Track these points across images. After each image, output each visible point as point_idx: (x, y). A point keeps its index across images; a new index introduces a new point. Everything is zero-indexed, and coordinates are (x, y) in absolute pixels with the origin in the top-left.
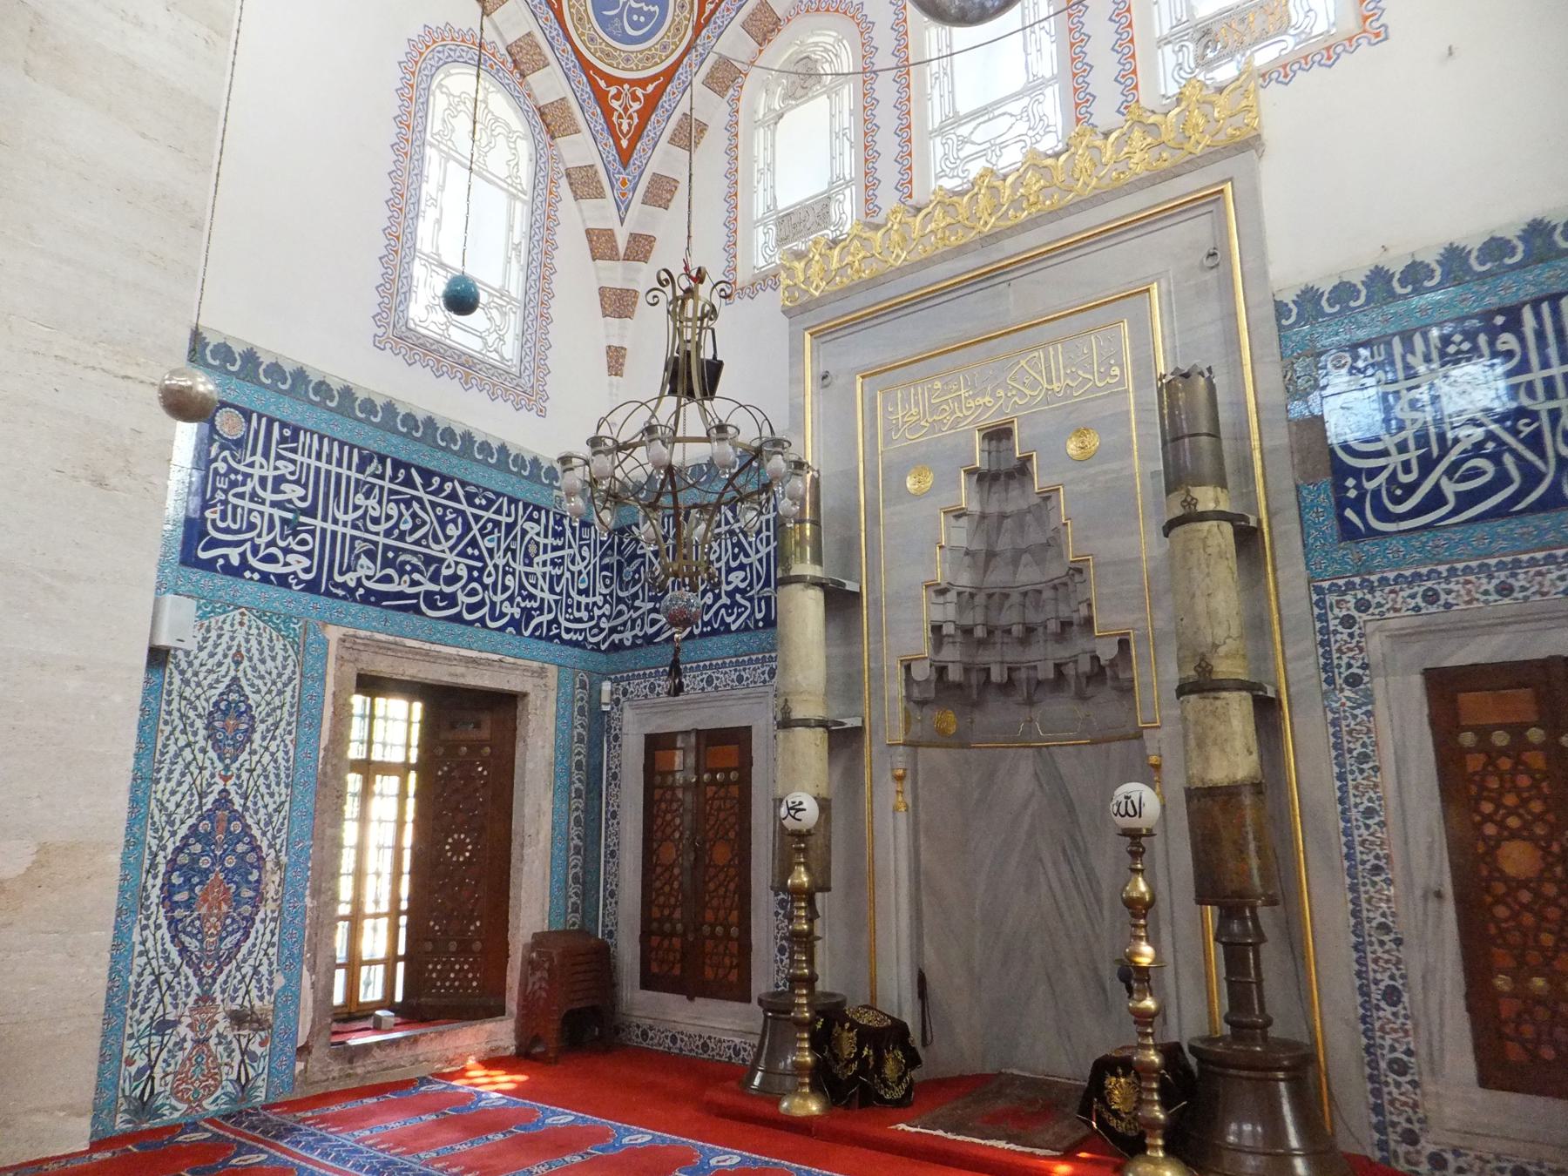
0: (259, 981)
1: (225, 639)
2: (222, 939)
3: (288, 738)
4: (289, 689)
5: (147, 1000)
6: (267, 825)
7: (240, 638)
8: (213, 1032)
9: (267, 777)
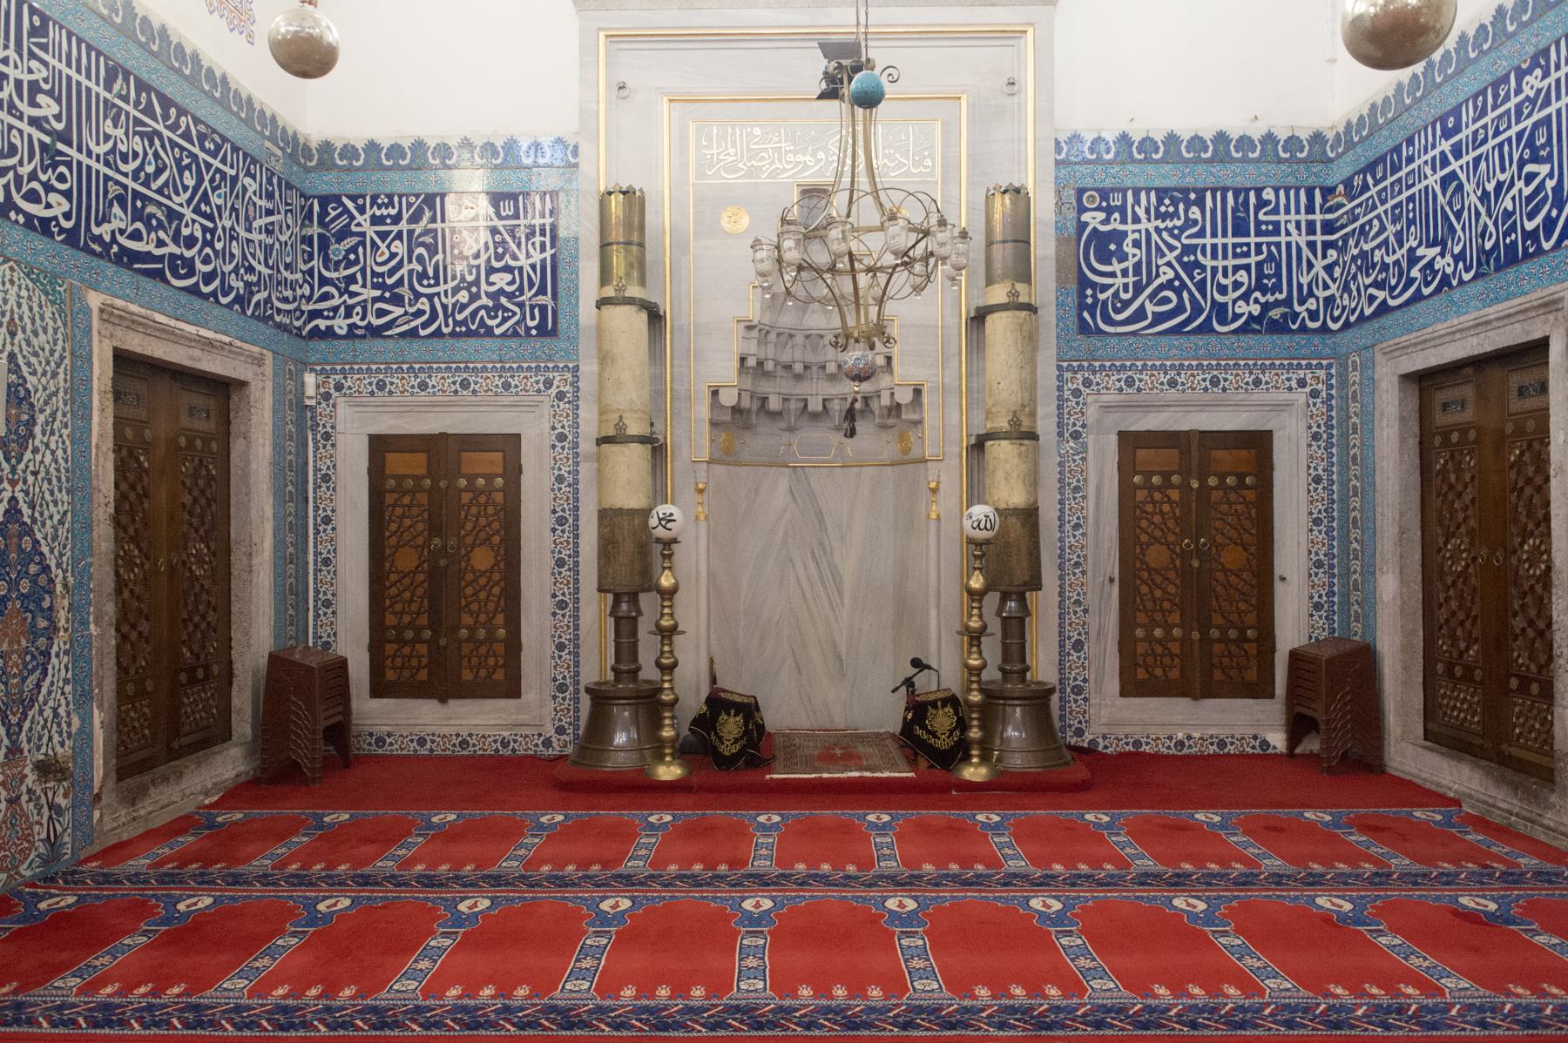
0: (59, 725)
4: (61, 370)
6: (54, 540)
8: (24, 789)
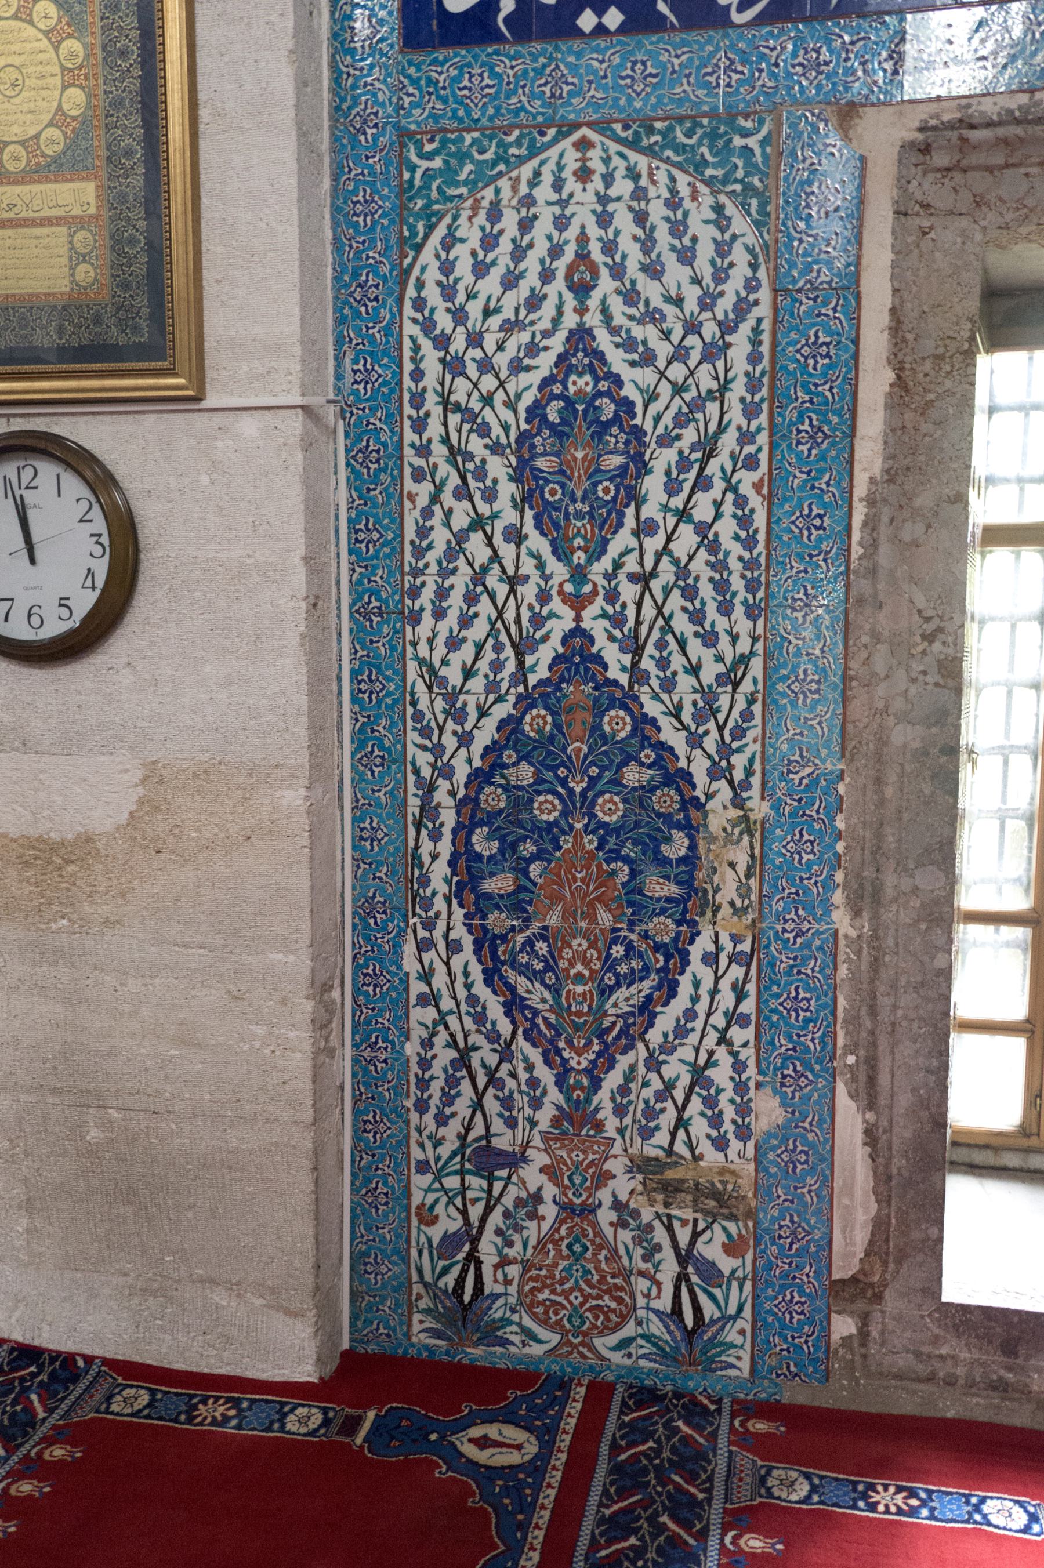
1: (544, 226)
2: (606, 992)
3: (746, 479)
5: (448, 1099)
7: (583, 216)
9: (690, 593)
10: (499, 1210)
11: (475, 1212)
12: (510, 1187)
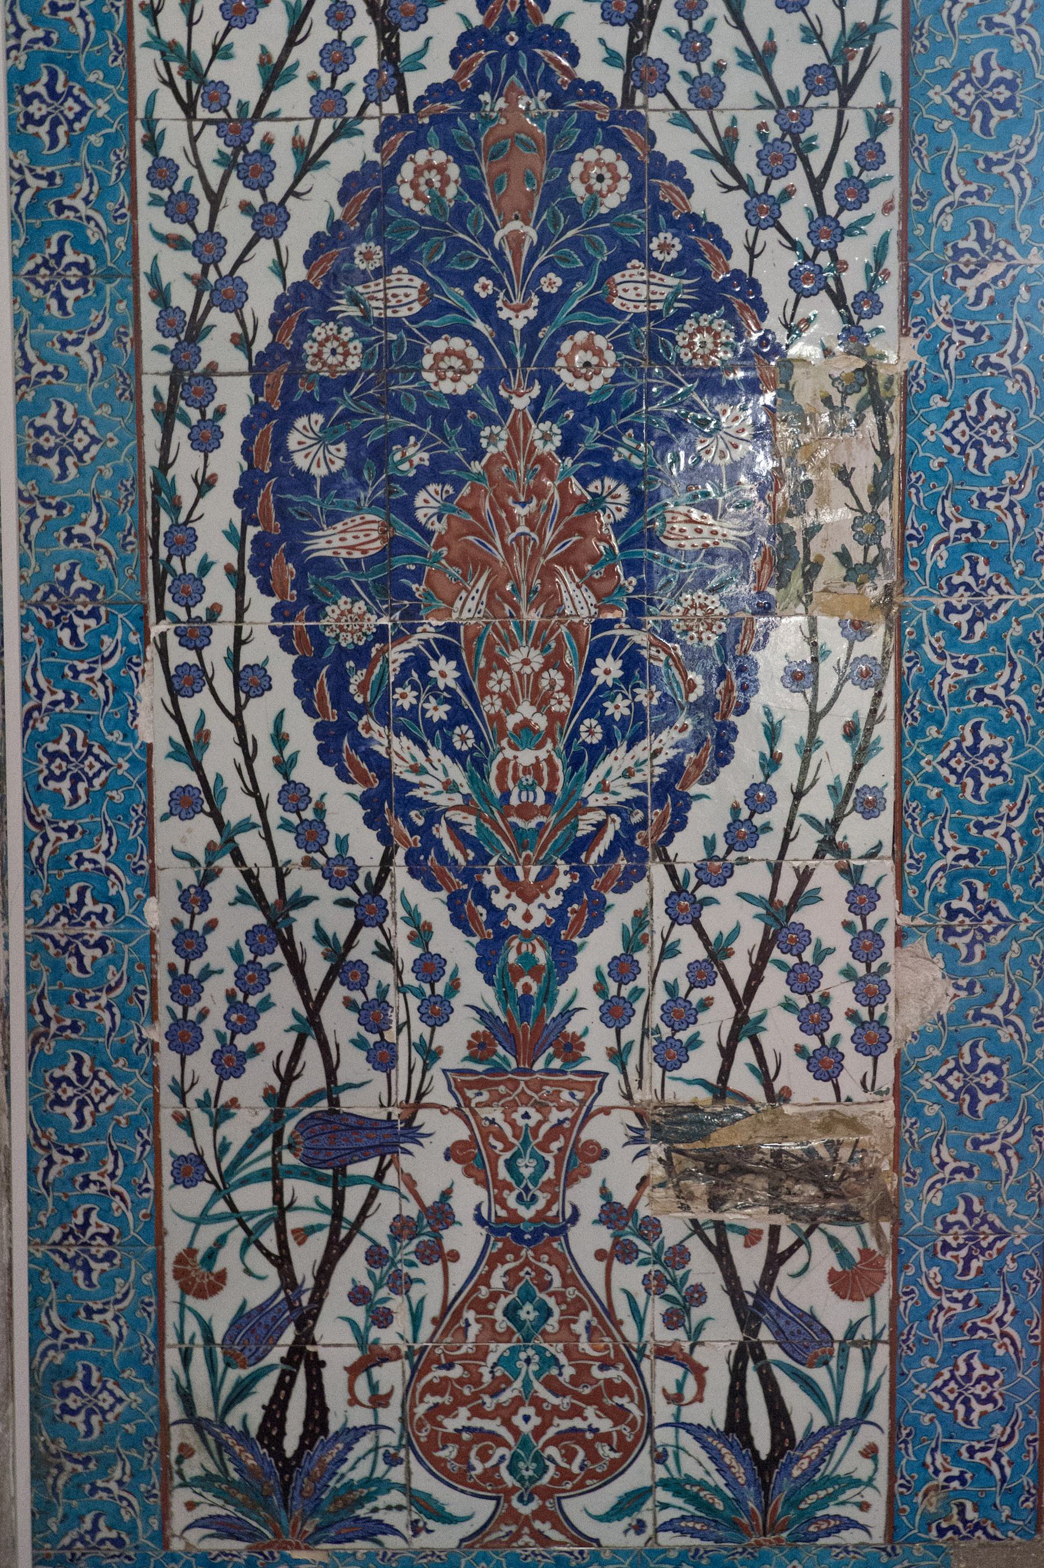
10: (358, 1247)
11: (306, 1259)
12: (383, 1196)
